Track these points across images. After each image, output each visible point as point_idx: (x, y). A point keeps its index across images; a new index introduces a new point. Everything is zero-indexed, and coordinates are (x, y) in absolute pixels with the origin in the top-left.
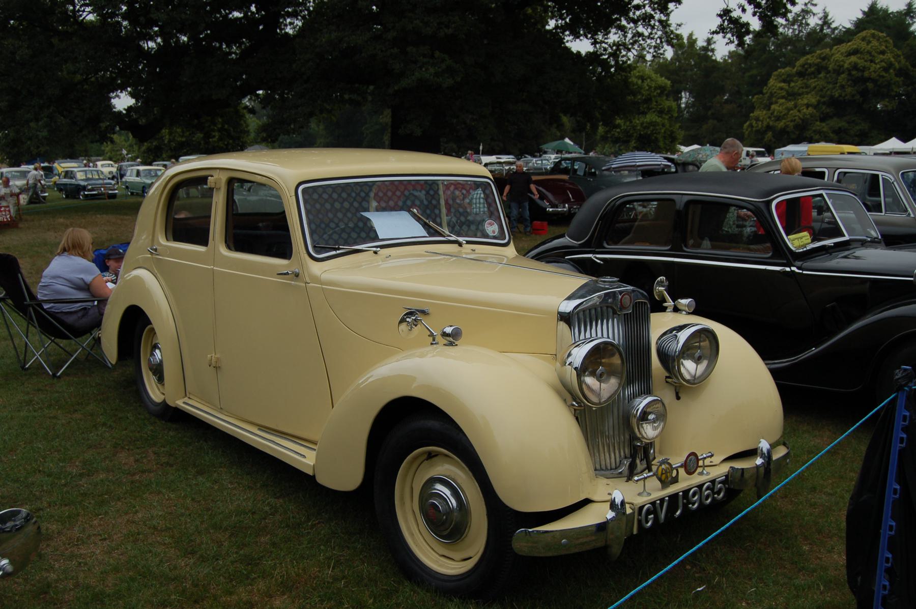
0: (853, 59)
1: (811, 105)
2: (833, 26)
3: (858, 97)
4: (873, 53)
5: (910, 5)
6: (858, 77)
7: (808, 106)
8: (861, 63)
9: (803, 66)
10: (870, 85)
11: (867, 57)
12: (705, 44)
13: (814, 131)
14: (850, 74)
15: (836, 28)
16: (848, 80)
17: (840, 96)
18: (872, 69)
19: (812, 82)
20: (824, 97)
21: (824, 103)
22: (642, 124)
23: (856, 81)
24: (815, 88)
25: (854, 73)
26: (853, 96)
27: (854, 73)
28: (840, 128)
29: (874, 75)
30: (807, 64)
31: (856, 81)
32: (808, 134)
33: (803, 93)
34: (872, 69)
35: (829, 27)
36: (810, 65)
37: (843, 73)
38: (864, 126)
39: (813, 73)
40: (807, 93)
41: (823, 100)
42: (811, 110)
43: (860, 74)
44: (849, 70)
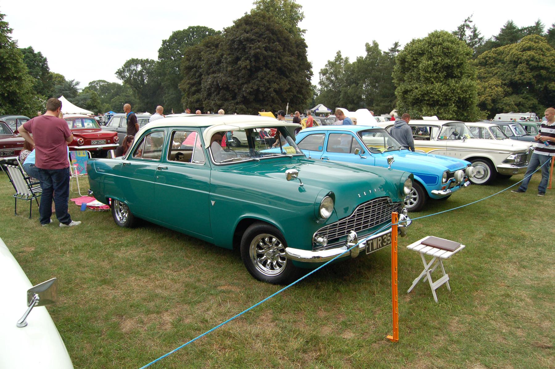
0: (529, 53)
1: (498, 86)
2: (480, 37)
3: (533, 80)
4: (544, 49)
5: (538, 24)
6: (535, 67)
7: (497, 86)
8: (537, 57)
9: (485, 58)
10: (543, 72)
11: (539, 52)
12: (393, 47)
13: (505, 104)
14: (527, 64)
15: (481, 38)
16: (527, 68)
17: (520, 79)
18: (546, 61)
19: (494, 70)
20: (505, 80)
21: (505, 84)
22: (461, 87)
23: (533, 69)
24: (497, 73)
25: (531, 62)
26: (530, 79)
27: (531, 62)
28: (520, 102)
29: (548, 65)
30: (487, 57)
31: (533, 69)
32: (499, 106)
33: (487, 78)
34: (546, 61)
35: (477, 37)
36: (490, 58)
37: (521, 63)
38: (535, 101)
39: (492, 63)
40: (491, 77)
41: (504, 82)
42: (500, 89)
43: (536, 64)
44: (527, 61)
